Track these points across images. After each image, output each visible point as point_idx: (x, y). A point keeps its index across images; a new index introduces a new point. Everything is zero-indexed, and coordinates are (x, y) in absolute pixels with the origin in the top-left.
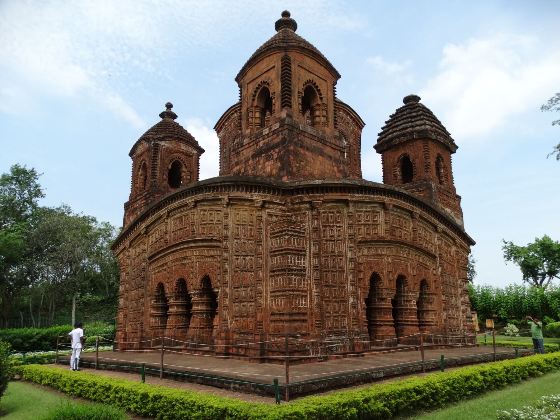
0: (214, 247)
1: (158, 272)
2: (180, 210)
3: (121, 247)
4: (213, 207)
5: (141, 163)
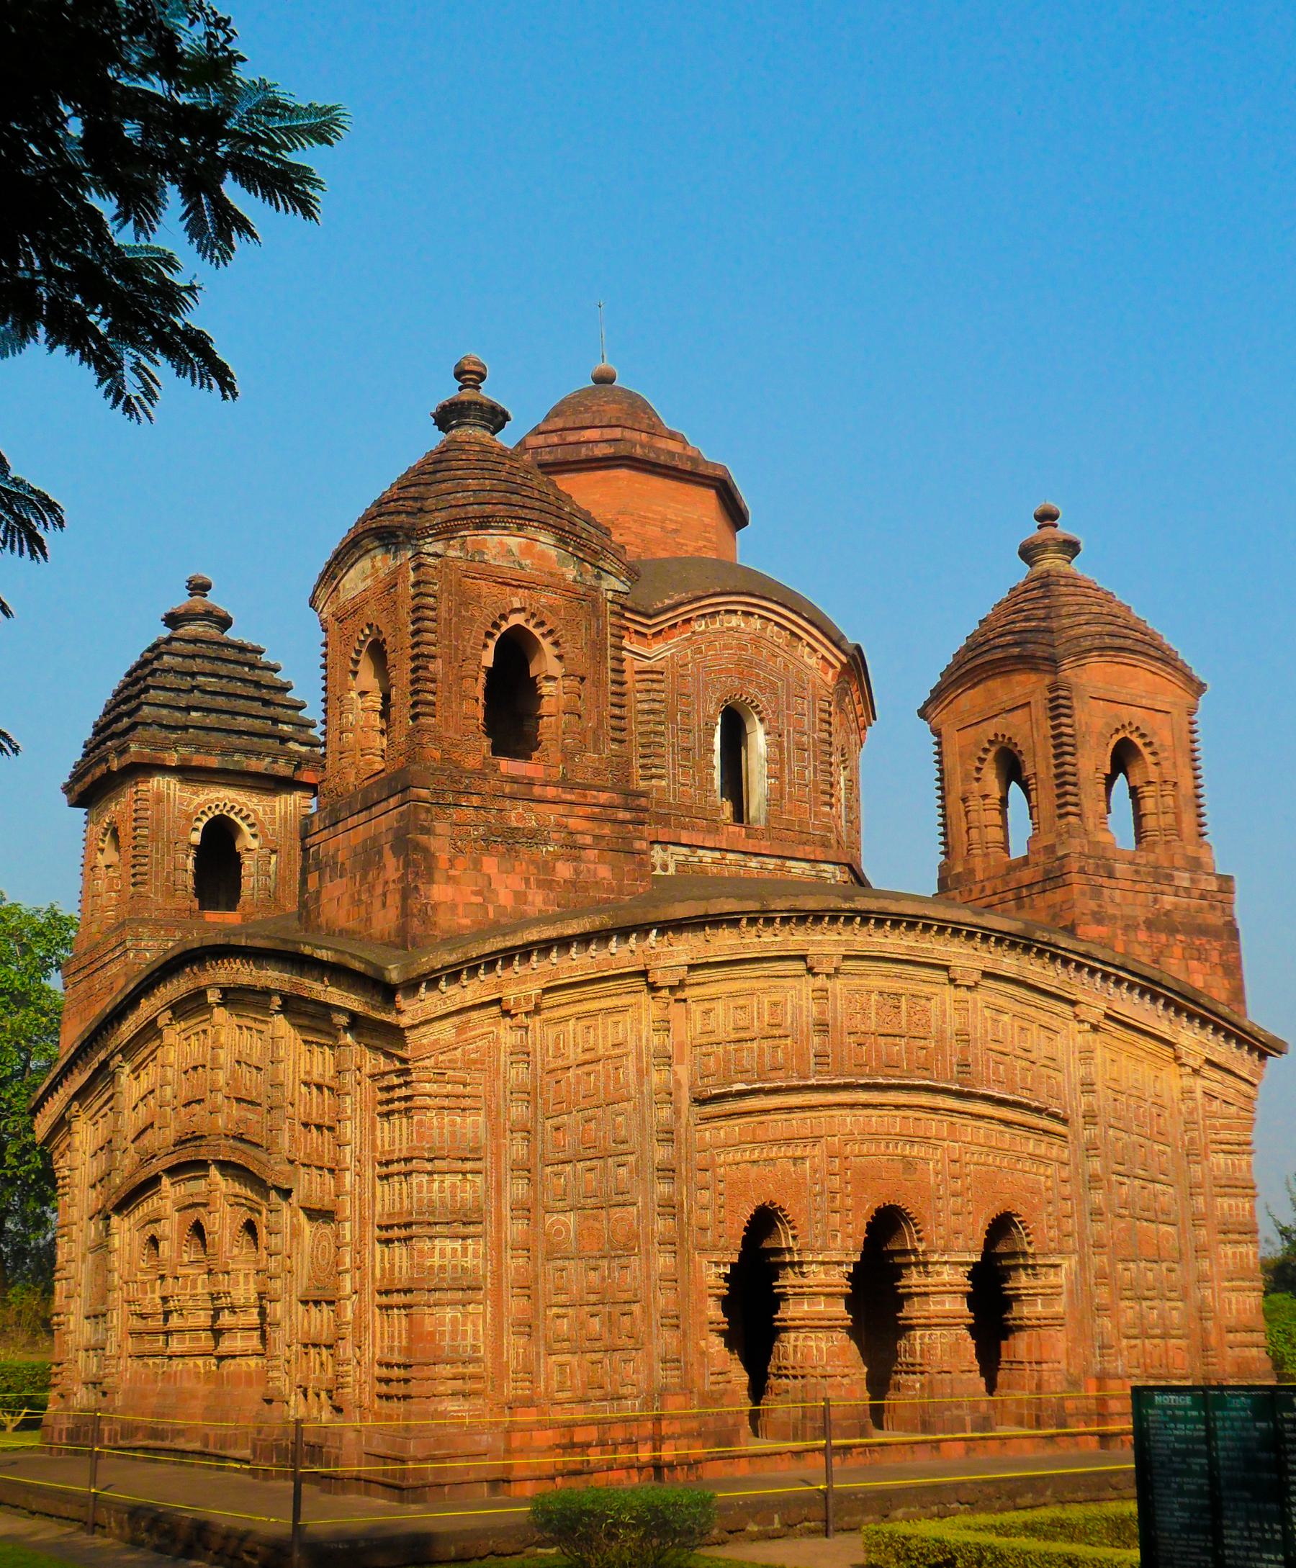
0: (1046, 1132)
4: (1031, 1011)
5: (504, 617)
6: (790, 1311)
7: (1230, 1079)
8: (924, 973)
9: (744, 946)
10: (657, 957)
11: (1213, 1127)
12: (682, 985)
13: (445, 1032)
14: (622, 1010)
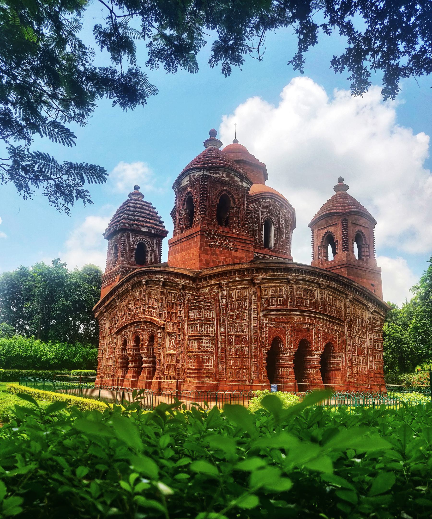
1: (274, 327)
2: (308, 283)
3: (213, 282)
6: (281, 362)
7: (379, 315)
8: (314, 285)
9: (275, 275)
10: (255, 276)
11: (374, 326)
12: (260, 283)
13: (206, 290)
14: (246, 288)
